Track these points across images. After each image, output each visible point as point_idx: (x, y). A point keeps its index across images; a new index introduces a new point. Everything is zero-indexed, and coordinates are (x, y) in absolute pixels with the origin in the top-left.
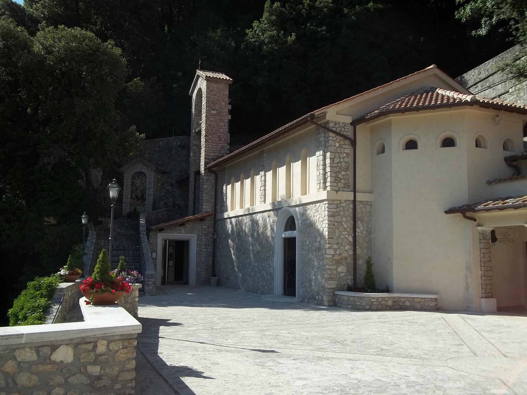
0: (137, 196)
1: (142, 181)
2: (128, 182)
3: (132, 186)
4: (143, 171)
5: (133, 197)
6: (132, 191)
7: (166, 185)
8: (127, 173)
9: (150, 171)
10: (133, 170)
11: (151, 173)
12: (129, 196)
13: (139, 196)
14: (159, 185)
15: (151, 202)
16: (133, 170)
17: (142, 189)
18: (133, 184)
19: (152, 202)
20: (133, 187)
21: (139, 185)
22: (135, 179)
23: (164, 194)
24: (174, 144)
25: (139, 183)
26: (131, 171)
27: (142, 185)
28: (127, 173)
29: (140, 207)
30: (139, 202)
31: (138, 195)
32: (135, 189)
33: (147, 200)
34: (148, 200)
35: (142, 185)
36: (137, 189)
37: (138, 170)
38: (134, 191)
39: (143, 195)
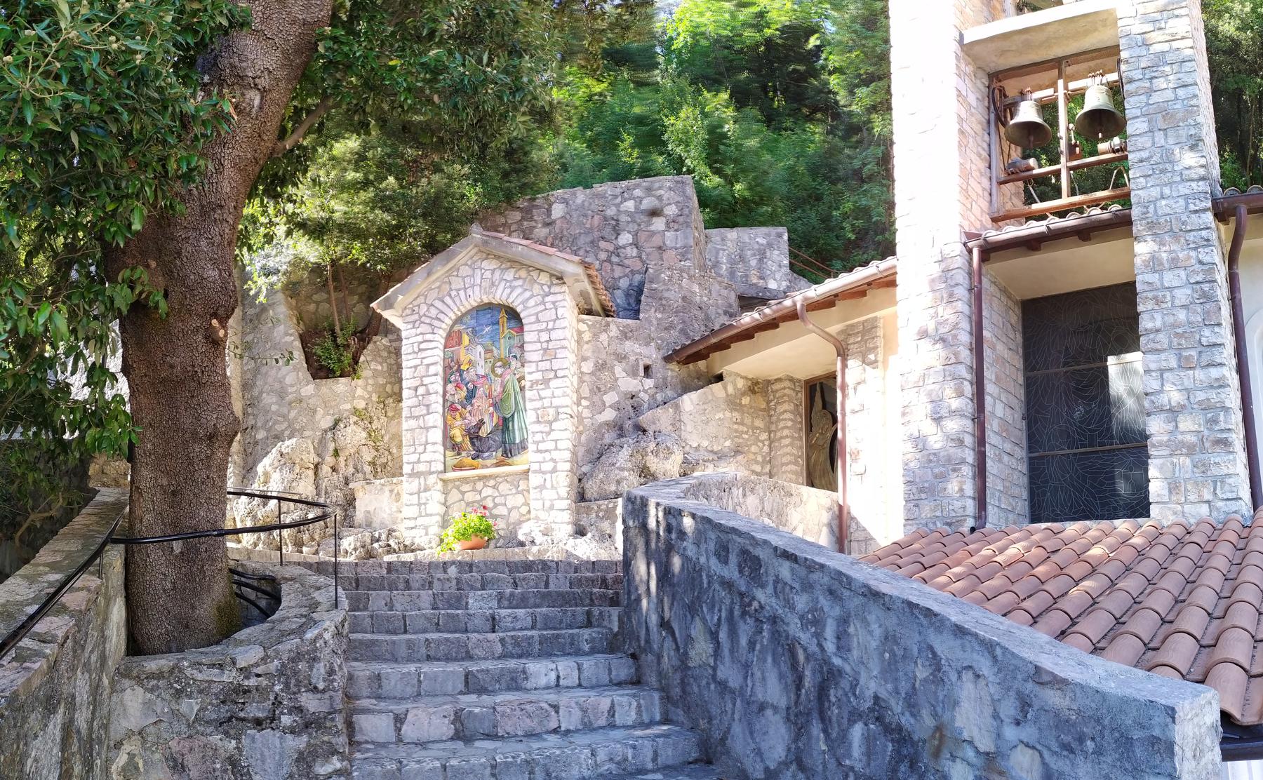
0: (473, 435)
1: (496, 352)
2: (426, 361)
3: (446, 381)
4: (500, 295)
5: (452, 438)
6: (450, 408)
7: (619, 370)
8: (416, 317)
9: (545, 288)
10: (448, 300)
11: (547, 299)
12: (437, 435)
13: (486, 430)
14: (588, 367)
15: (555, 455)
16: (448, 300)
17: (499, 389)
18: (452, 370)
19: (568, 455)
20: (450, 387)
21: (481, 372)
22: (460, 343)
23: (609, 415)
24: (623, 207)
25: (482, 363)
26: (438, 304)
27: (499, 371)
28: (416, 317)
29: (494, 487)
30: (489, 462)
31: (481, 422)
32: (464, 393)
33: (537, 443)
34: (542, 447)
35: (499, 371)
36: (471, 395)
37: (476, 297)
38: (459, 407)
39: (505, 425)
